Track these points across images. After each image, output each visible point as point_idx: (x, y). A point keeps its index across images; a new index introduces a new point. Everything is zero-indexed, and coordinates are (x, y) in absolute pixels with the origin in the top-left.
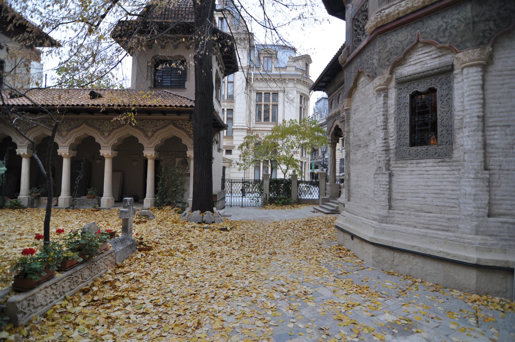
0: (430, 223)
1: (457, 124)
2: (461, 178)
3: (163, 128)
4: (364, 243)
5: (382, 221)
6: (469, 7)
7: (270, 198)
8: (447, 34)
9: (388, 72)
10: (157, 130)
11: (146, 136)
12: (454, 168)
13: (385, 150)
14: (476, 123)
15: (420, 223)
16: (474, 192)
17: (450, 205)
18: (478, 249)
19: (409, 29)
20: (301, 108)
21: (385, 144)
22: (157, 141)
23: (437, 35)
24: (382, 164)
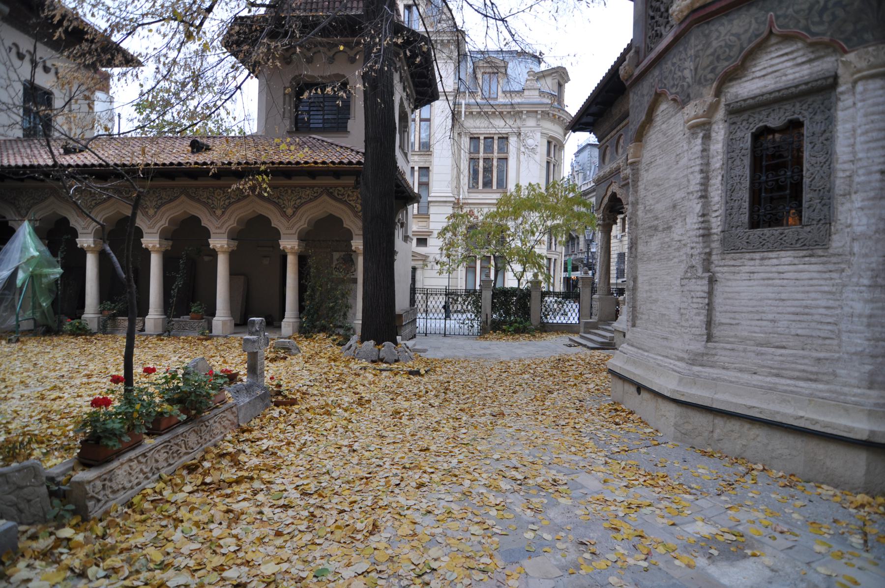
0: (783, 366)
1: (840, 185)
2: (844, 286)
3: (311, 200)
4: (660, 400)
5: (693, 362)
7: (493, 321)
8: (826, 17)
9: (712, 92)
10: (302, 204)
11: (284, 214)
12: (831, 267)
13: (703, 236)
14: (878, 185)
15: (764, 367)
17: (822, 335)
18: (871, 414)
19: (753, 10)
20: (548, 163)
21: (703, 225)
22: (302, 222)
23: (807, 19)
24: (697, 261)
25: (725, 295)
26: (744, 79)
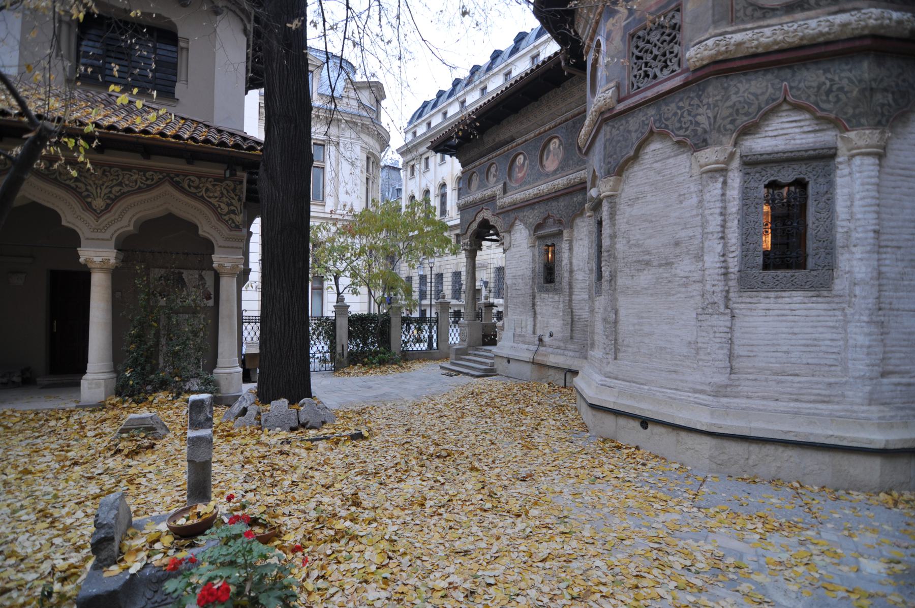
1: (840, 239)
2: (849, 322)
3: (140, 190)
4: (683, 434)
5: (716, 394)
6: (865, 65)
7: (351, 353)
9: (732, 142)
10: (123, 195)
11: (88, 207)
12: (834, 306)
13: (725, 274)
14: (872, 241)
15: (784, 393)
16: (867, 343)
19: (769, 76)
20: (367, 179)
23: (816, 96)
24: (719, 298)
25: (743, 330)
26: (757, 136)
